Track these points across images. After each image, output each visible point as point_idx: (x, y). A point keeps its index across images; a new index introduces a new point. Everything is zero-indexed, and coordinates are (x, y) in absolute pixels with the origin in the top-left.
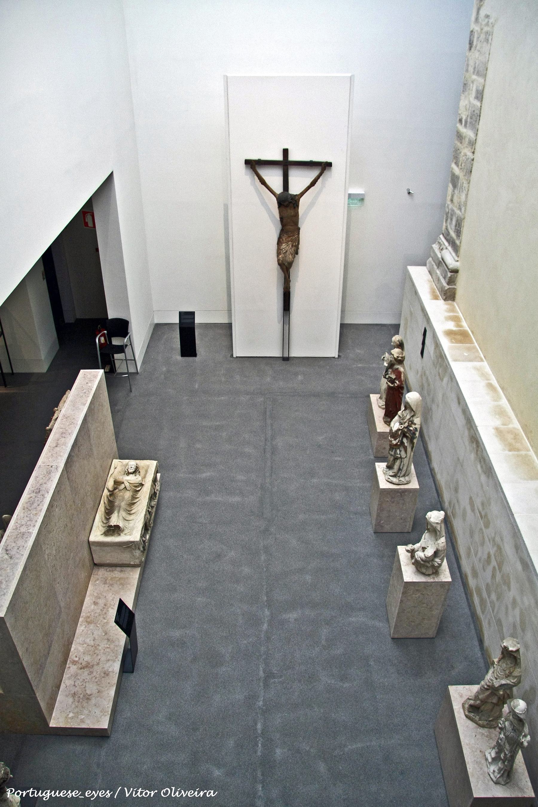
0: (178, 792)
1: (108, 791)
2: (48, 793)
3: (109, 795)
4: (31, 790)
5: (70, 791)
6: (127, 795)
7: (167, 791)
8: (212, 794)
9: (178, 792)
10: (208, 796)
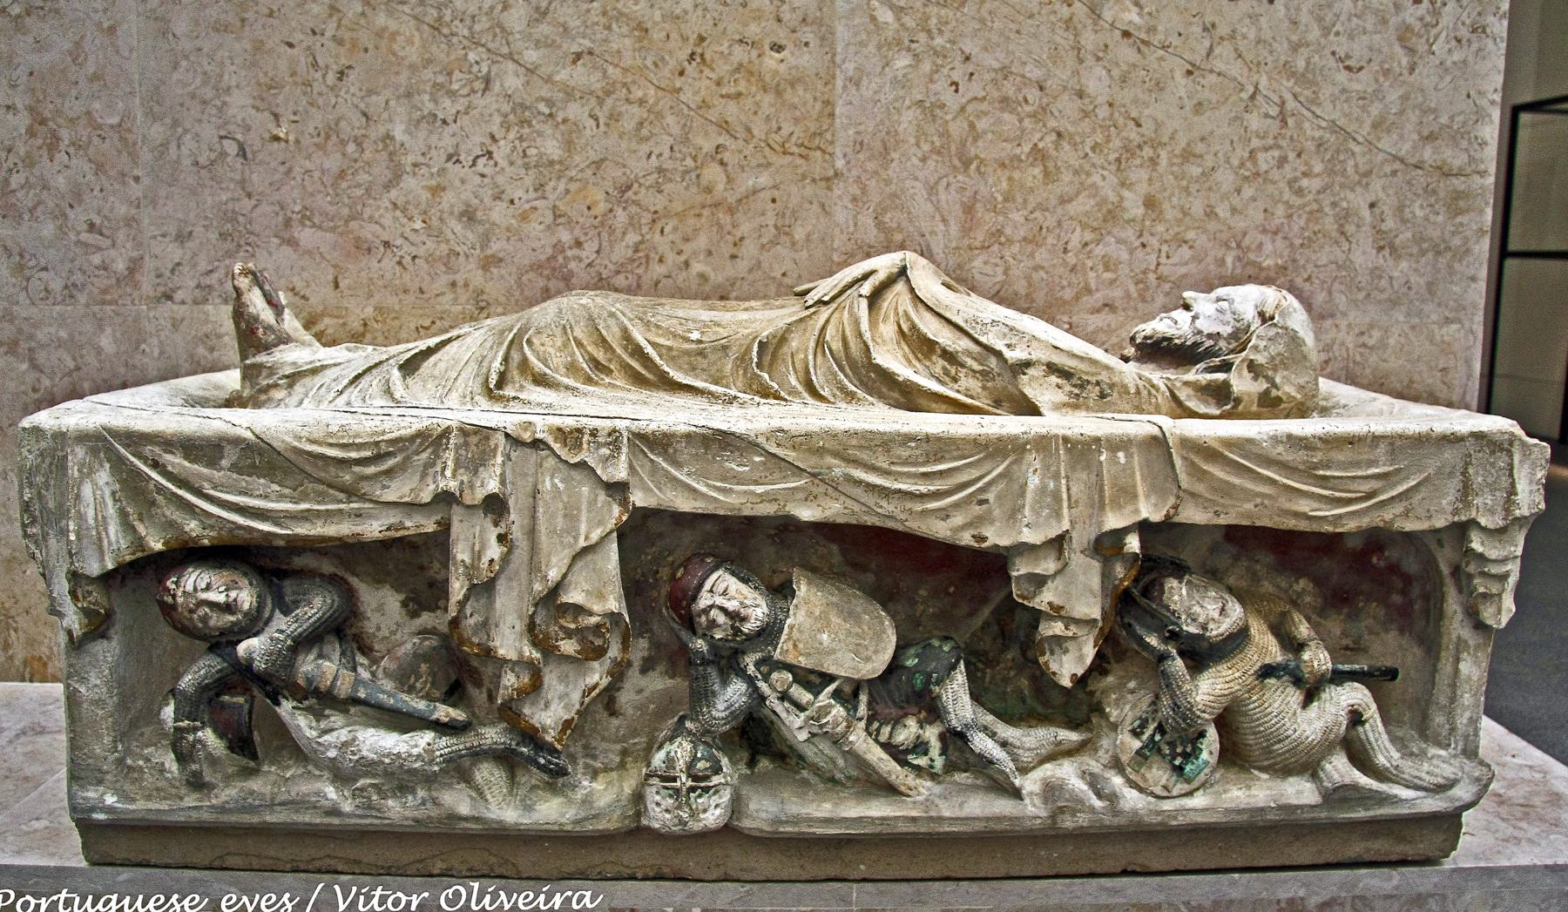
0: (488, 897)
1: (287, 895)
2: (113, 903)
3: (289, 906)
4: (64, 895)
5: (176, 896)
6: (342, 907)
7: (457, 894)
8: (587, 900)
9: (488, 897)
10: (575, 906)
